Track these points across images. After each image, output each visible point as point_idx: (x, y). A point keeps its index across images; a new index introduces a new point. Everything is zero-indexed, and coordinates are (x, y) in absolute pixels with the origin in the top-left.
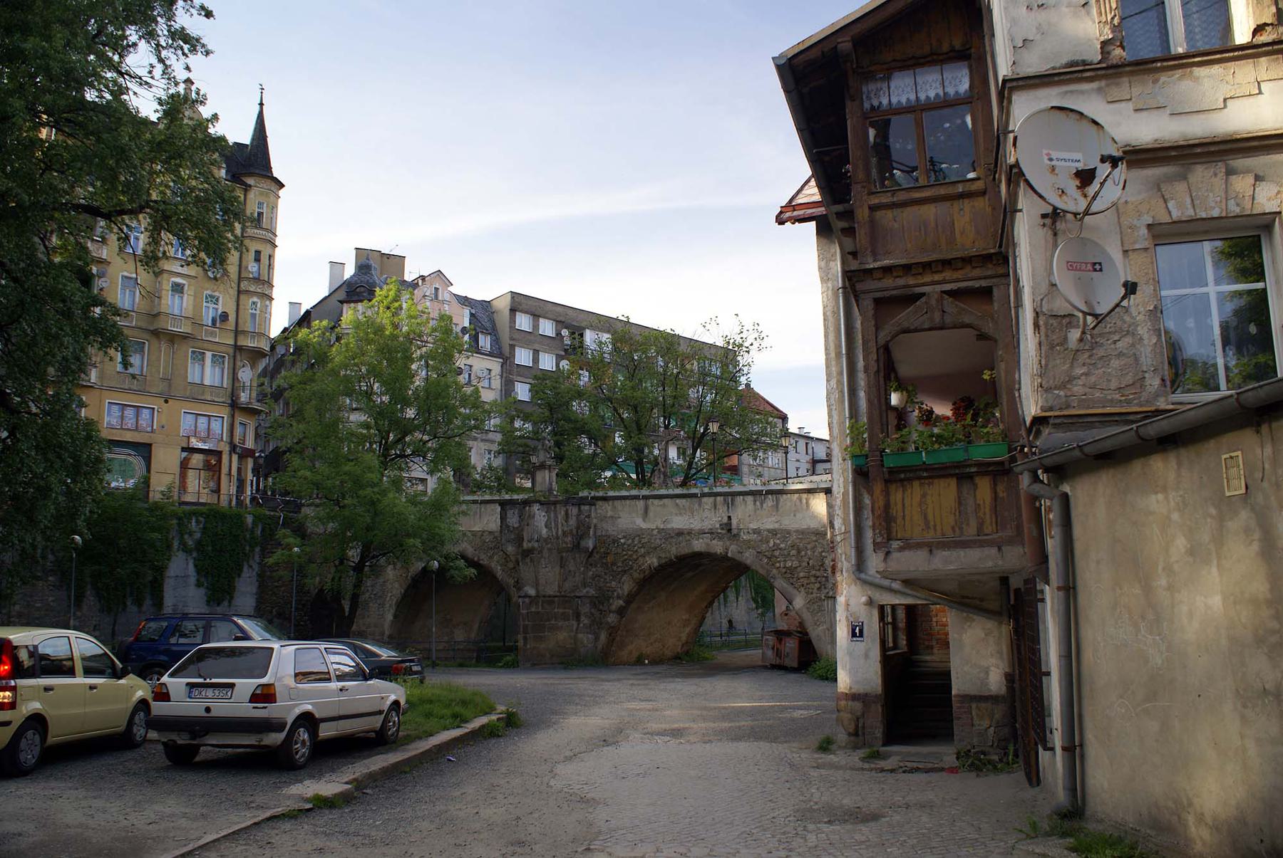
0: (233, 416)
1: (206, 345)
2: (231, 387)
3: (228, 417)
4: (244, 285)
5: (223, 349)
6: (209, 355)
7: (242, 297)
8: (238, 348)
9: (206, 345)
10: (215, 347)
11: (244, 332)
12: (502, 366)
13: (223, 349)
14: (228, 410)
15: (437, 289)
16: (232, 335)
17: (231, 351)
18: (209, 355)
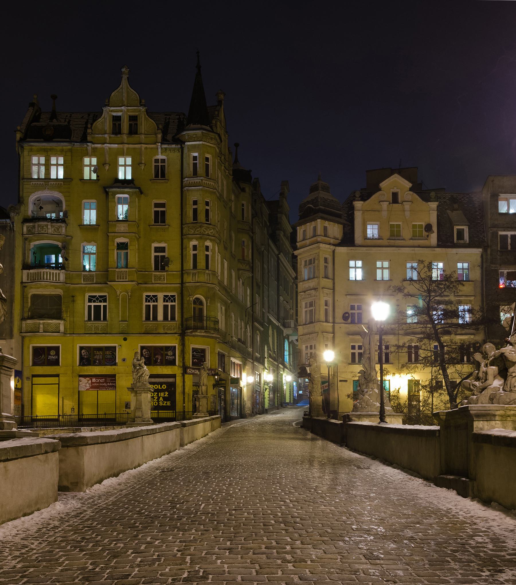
2: (180, 319)
3: (179, 345)
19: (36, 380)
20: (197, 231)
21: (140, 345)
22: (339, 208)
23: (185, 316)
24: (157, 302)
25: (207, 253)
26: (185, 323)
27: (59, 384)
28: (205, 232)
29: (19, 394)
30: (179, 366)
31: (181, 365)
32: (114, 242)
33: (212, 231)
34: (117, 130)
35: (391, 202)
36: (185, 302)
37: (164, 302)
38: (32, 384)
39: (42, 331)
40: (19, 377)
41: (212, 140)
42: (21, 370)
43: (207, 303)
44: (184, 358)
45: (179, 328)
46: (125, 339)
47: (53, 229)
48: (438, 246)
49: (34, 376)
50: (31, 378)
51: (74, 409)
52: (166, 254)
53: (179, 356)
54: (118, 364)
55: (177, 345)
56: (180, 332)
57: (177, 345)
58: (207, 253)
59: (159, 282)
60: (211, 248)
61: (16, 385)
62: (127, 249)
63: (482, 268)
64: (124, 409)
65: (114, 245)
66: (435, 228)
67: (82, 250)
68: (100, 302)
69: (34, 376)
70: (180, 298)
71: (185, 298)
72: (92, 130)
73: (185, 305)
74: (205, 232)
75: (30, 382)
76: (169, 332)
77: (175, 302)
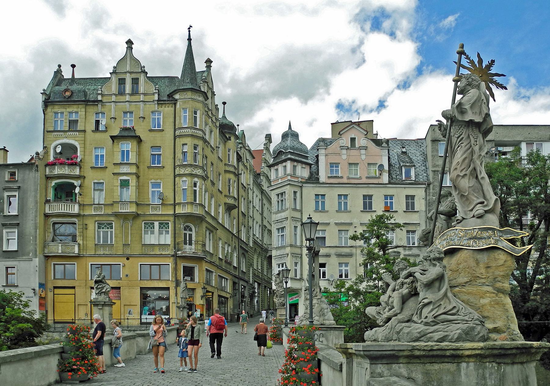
0: (176, 264)
1: (153, 218)
2: (173, 243)
4: (178, 171)
5: (166, 218)
6: (156, 224)
7: (177, 179)
8: (176, 216)
9: (153, 218)
10: (160, 218)
11: (179, 204)
12: (426, 191)
13: (166, 218)
14: (172, 259)
15: (353, 140)
16: (172, 207)
17: (172, 219)
18: (156, 224)
19: (57, 291)
20: (187, 171)
21: (140, 263)
22: (306, 151)
23: (177, 241)
24: (154, 228)
25: (195, 188)
26: (177, 246)
27: (75, 294)
28: (193, 171)
29: (43, 302)
30: (172, 281)
31: (174, 280)
32: (118, 179)
33: (199, 171)
34: (121, 93)
35: (350, 146)
36: (177, 228)
37: (160, 228)
38: (54, 294)
39: (61, 252)
40: (43, 288)
41: (199, 97)
42: (44, 283)
43: (195, 230)
44: (176, 274)
45: (172, 250)
46: (128, 259)
47: (69, 170)
48: (390, 183)
49: (55, 288)
50: (53, 289)
51: (87, 314)
52: (161, 190)
53: (172, 273)
54: (122, 279)
55: (170, 264)
56: (173, 253)
57: (170, 264)
58: (195, 188)
59: (155, 213)
60: (198, 185)
61: (41, 295)
62: (129, 186)
63: (426, 200)
64: (128, 315)
65: (118, 182)
66: (386, 167)
67: (93, 187)
68: (108, 228)
69: (55, 288)
70: (173, 225)
71: (176, 226)
72: (102, 91)
73: (177, 232)
74: (193, 171)
75: (52, 293)
76: (164, 253)
77: (169, 228)
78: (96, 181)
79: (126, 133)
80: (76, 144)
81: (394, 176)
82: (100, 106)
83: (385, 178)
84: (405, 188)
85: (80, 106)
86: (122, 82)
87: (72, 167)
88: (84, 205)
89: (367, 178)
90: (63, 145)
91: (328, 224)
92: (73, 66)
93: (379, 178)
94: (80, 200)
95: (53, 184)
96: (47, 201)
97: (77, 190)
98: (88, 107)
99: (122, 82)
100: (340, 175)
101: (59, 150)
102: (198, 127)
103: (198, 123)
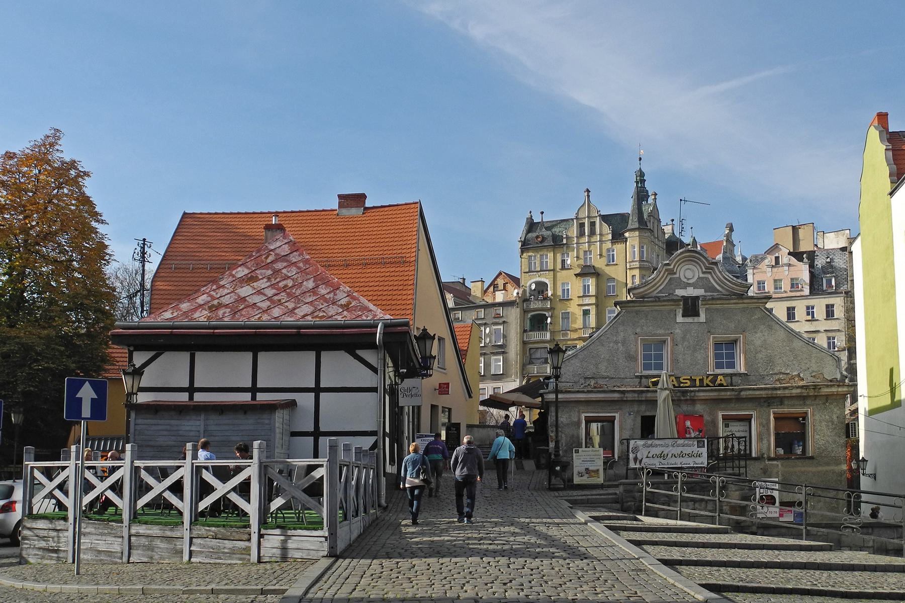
78: (563, 311)
79: (586, 271)
80: (547, 281)
81: (816, 287)
82: (565, 248)
83: (807, 291)
84: (824, 298)
85: (549, 249)
86: (582, 226)
87: (544, 302)
88: (554, 332)
89: (791, 291)
90: (537, 283)
91: (818, 332)
92: (542, 213)
93: (802, 291)
94: (551, 328)
95: (529, 316)
96: (525, 331)
97: (549, 320)
98: (556, 249)
99: (582, 226)
100: (766, 291)
101: (533, 287)
102: (645, 259)
103: (645, 256)
